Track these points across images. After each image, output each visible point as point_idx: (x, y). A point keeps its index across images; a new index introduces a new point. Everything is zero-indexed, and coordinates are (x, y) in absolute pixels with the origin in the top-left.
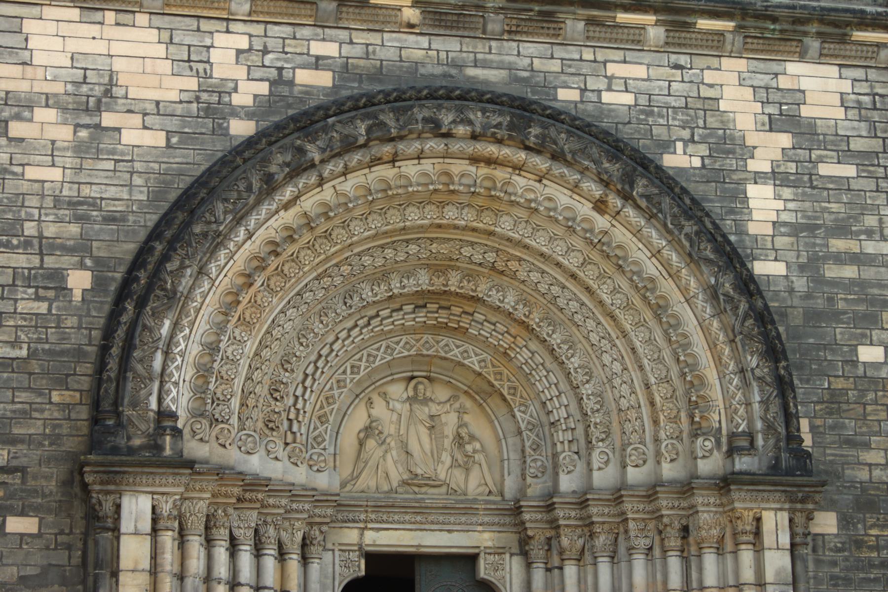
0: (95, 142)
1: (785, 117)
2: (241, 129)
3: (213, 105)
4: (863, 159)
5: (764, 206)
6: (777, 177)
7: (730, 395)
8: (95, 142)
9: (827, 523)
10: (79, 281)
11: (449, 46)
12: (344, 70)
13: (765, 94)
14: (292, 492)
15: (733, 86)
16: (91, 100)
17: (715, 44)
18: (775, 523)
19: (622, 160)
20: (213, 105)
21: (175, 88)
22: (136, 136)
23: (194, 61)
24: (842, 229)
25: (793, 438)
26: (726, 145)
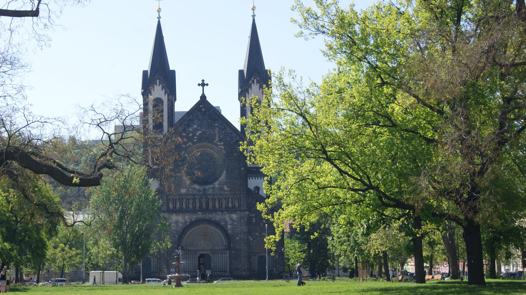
0: (177, 226)
1: (231, 219)
2: (188, 224)
3: (186, 222)
4: (238, 222)
5: (229, 227)
6: (230, 224)
7: (225, 242)
8: (177, 226)
9: (233, 252)
10: (176, 236)
11: (204, 216)
12: (196, 218)
13: (230, 218)
14: (193, 250)
15: (227, 217)
16: (177, 222)
17: (225, 214)
18: (228, 252)
19: (217, 224)
20: (186, 222)
21: (183, 221)
22: (180, 225)
23: (184, 219)
24: (236, 228)
25: (230, 245)
26: (226, 222)
